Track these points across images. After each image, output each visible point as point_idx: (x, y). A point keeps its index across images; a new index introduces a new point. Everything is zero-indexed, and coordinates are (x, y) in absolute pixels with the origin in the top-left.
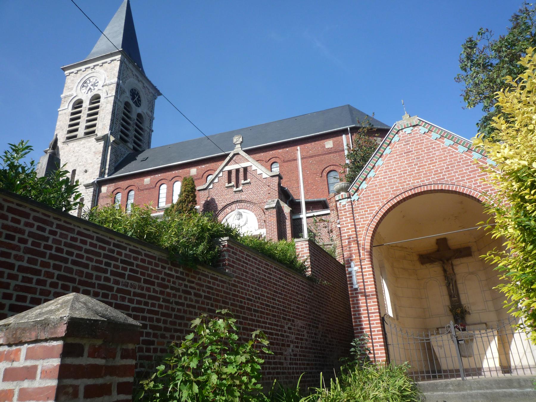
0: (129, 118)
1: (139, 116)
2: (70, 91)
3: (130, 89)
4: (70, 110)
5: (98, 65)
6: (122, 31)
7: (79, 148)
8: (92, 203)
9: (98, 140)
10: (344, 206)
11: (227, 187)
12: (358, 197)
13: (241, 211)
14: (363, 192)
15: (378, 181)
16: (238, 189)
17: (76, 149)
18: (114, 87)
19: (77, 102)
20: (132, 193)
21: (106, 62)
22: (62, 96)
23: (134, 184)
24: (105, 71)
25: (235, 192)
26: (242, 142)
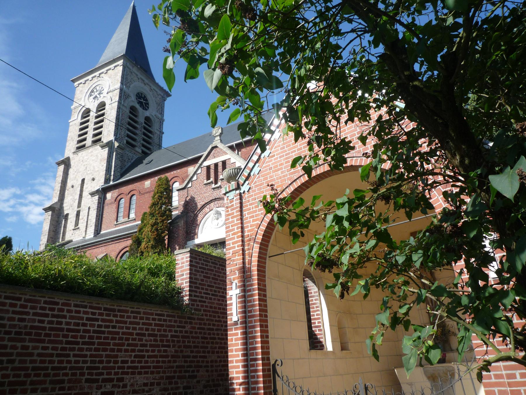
0: (136, 122)
1: (147, 119)
3: (136, 94)
4: (79, 120)
5: (102, 73)
6: (127, 37)
7: (87, 157)
8: (97, 211)
9: (103, 147)
10: (232, 201)
11: (205, 184)
12: (249, 186)
13: (219, 209)
14: (255, 180)
15: (273, 161)
16: (217, 186)
17: (86, 158)
18: (117, 92)
19: (86, 112)
20: (134, 198)
21: (110, 69)
22: (72, 107)
23: (135, 189)
24: (110, 77)
25: (214, 189)
26: (221, 134)
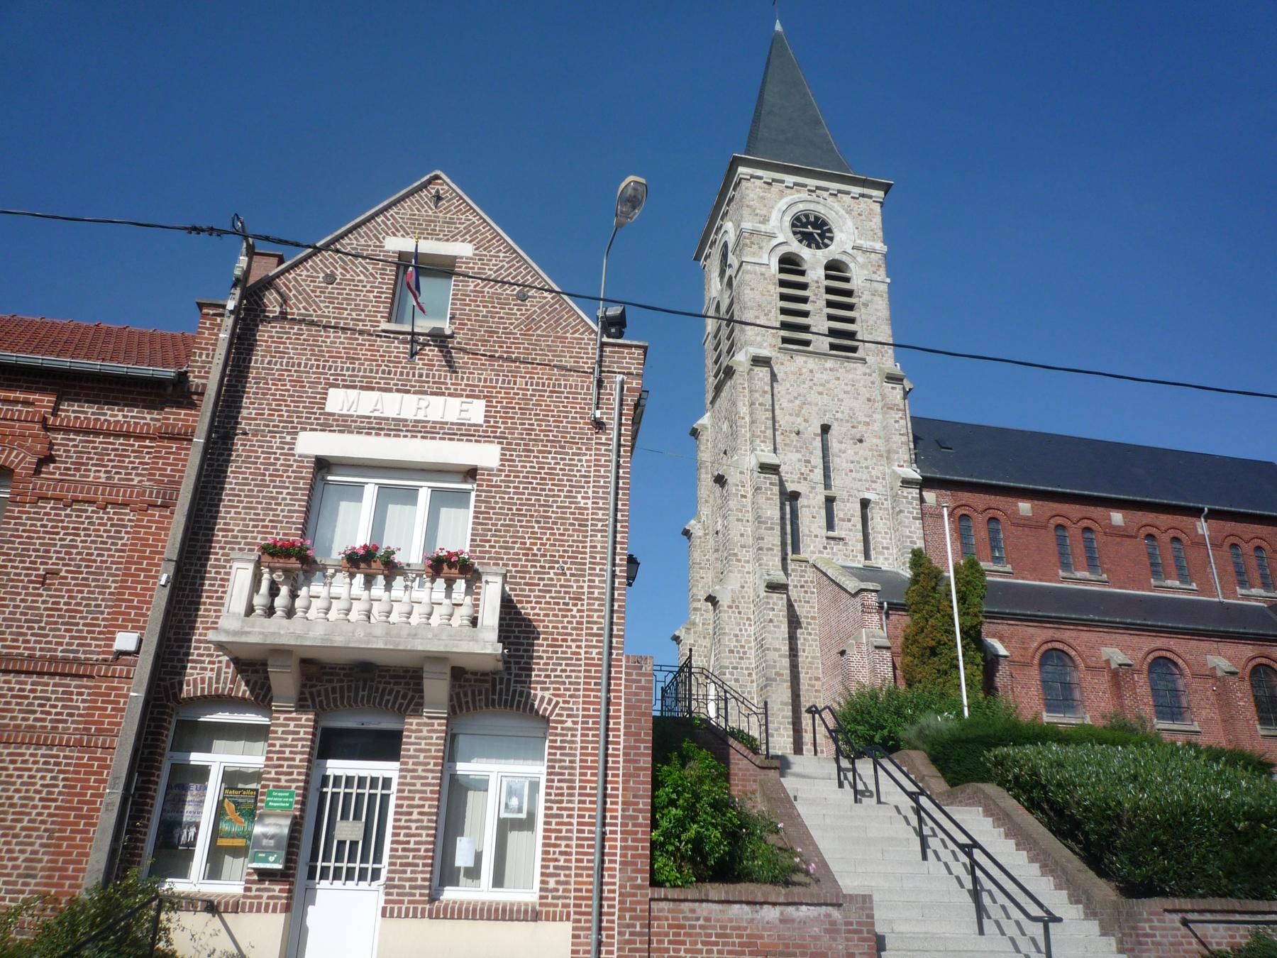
2: (760, 222)
7: (825, 377)
17: (818, 375)
21: (848, 193)
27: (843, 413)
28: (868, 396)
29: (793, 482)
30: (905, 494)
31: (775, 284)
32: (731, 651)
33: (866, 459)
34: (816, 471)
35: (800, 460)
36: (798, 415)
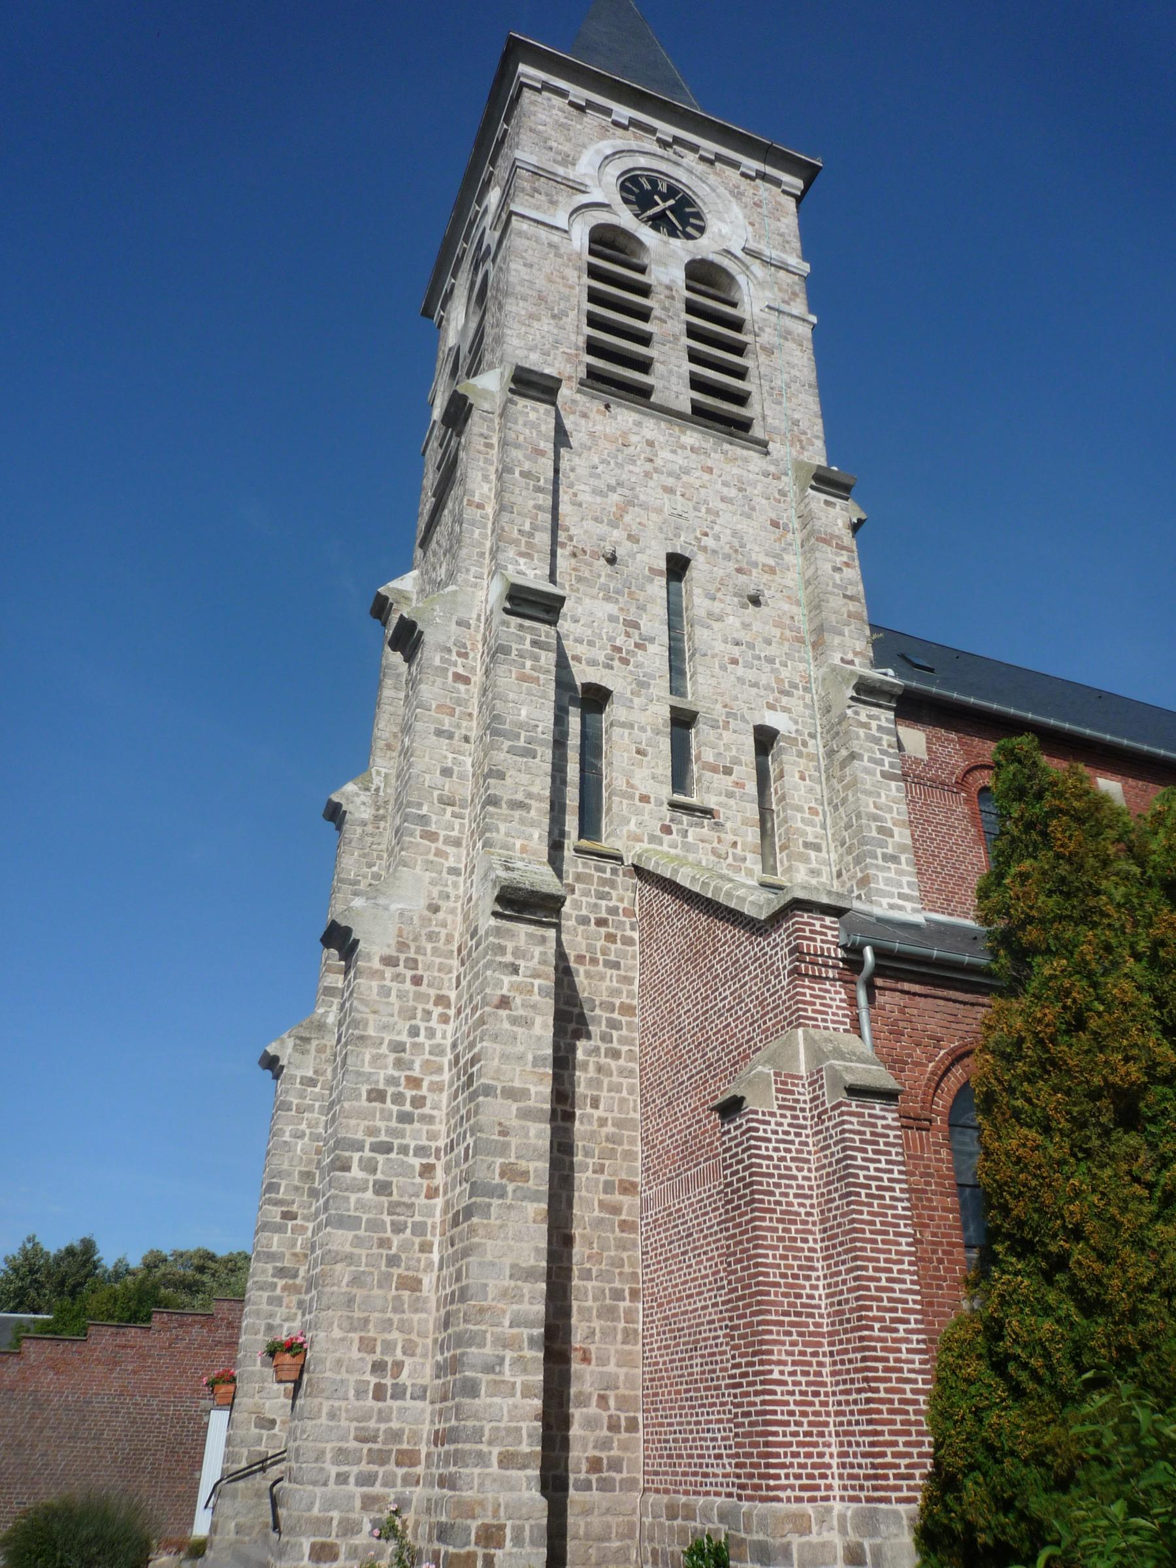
7: (680, 460)
17: (664, 455)
27: (717, 538)
28: (774, 516)
29: (593, 663)
30: (863, 718)
31: (579, 269)
32: (377, 1095)
33: (768, 642)
34: (652, 648)
35: (612, 619)
36: (614, 524)
